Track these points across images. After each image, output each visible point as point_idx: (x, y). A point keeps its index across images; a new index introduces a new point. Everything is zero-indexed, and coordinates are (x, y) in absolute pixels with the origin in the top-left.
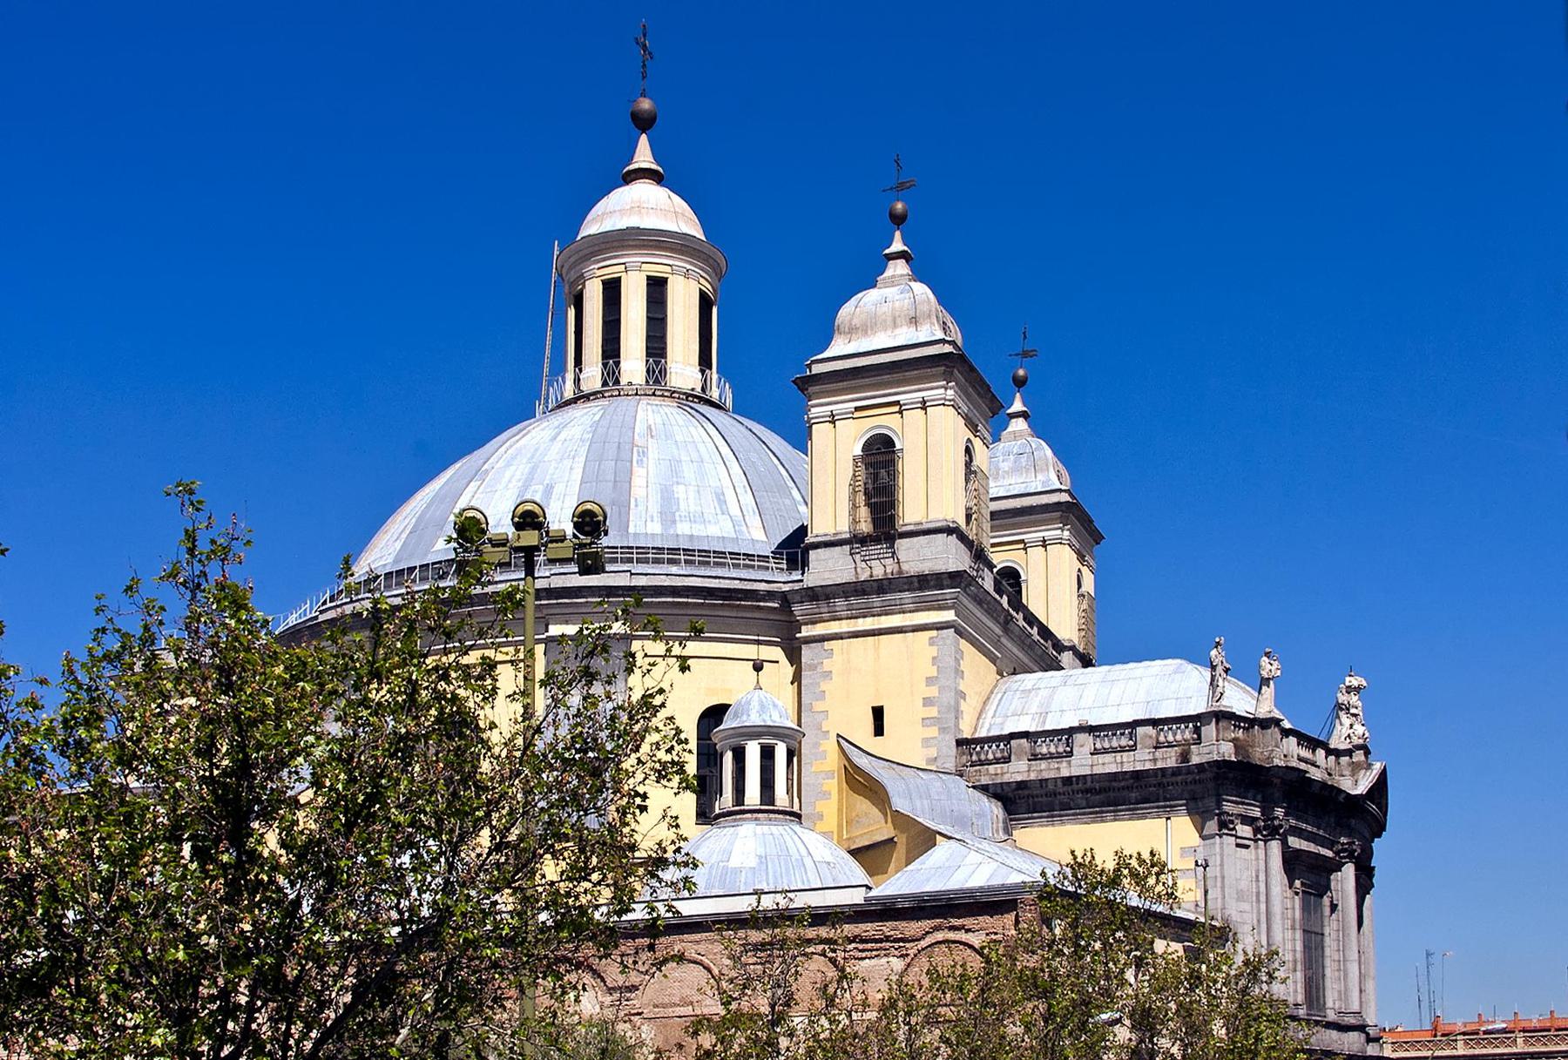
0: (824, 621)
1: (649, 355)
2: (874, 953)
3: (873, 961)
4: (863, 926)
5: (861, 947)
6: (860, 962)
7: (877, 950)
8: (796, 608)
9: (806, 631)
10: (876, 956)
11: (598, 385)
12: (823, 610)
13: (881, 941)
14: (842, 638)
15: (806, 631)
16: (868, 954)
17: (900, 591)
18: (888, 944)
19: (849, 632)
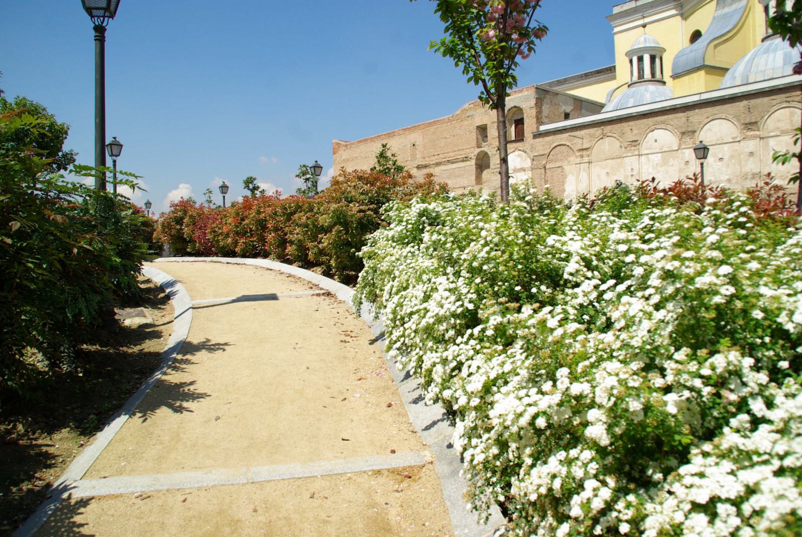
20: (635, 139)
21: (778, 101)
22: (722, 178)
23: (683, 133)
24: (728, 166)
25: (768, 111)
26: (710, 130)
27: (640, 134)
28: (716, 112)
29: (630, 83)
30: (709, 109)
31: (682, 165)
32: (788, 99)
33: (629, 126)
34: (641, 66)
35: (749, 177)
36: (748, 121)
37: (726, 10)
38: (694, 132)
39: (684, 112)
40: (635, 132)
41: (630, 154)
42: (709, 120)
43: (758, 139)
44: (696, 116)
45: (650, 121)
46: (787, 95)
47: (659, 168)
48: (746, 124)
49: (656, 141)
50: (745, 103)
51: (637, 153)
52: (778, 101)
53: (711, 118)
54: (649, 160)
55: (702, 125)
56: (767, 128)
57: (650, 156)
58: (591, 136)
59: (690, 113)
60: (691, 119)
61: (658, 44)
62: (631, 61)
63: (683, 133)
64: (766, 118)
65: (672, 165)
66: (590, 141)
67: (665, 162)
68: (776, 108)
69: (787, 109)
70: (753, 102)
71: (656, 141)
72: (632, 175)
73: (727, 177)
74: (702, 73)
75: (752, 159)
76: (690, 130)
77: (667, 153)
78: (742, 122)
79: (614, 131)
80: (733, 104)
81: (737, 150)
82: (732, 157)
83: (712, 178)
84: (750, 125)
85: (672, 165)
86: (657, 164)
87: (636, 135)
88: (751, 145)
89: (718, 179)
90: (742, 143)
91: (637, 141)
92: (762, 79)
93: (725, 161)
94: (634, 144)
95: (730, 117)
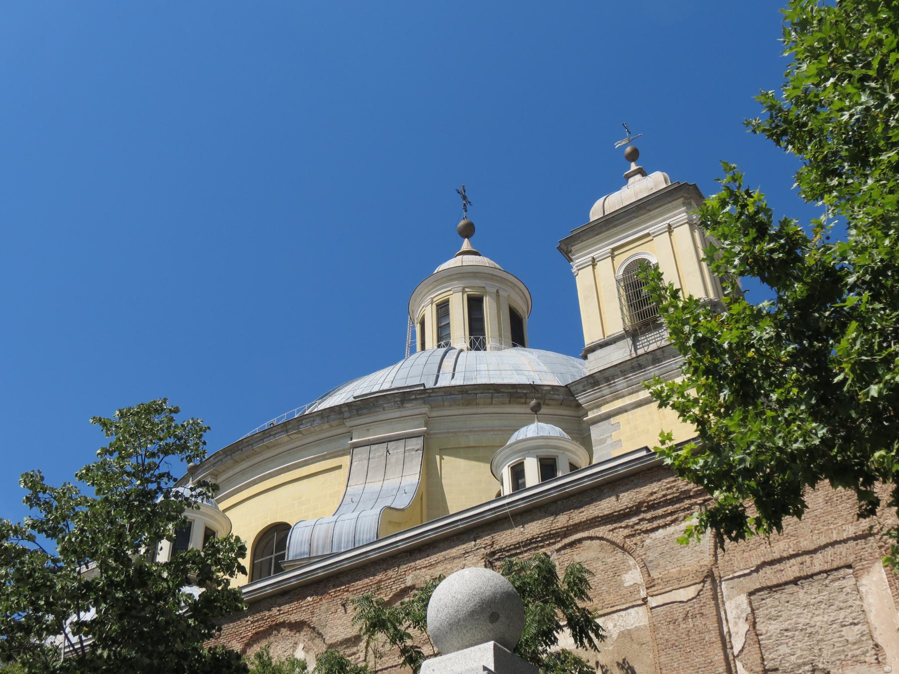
0: (608, 403)
1: (470, 334)
2: (669, 518)
3: (670, 530)
4: (646, 490)
5: (649, 515)
6: (653, 535)
7: (672, 513)
8: (582, 399)
9: (591, 415)
10: (673, 522)
12: (605, 392)
13: (678, 500)
14: (626, 411)
15: (591, 415)
16: (661, 522)
17: (674, 357)
18: (687, 503)
19: (631, 404)
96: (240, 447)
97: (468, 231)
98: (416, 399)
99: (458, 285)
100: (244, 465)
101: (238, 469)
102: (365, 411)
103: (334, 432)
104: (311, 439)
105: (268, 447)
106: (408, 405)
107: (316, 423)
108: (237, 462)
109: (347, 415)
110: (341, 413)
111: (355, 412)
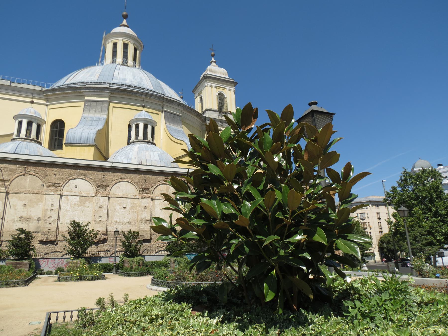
11: (121, 63)
20: (56, 182)
21: (161, 179)
22: (125, 221)
23: (99, 186)
24: (129, 213)
25: (156, 184)
26: (119, 187)
27: (63, 179)
28: (124, 177)
29: (14, 136)
30: (120, 174)
31: (97, 208)
32: (166, 180)
33: (53, 171)
34: (29, 128)
35: (143, 222)
36: (144, 187)
37: (91, 115)
38: (107, 186)
39: (101, 171)
40: (57, 176)
41: (53, 193)
42: (119, 180)
43: (150, 199)
44: (110, 176)
45: (73, 171)
46: (166, 177)
47: (76, 208)
48: (142, 188)
49: (76, 187)
50: (142, 176)
51: (59, 193)
52: (161, 179)
53: (121, 180)
54: (68, 200)
55: (113, 183)
56: (155, 194)
57: (69, 197)
58: (11, 170)
59: (106, 173)
60: (106, 177)
61: (41, 117)
62: (20, 123)
63: (99, 186)
64: (154, 187)
65: (88, 207)
66: (10, 175)
67: (82, 204)
68: (160, 183)
69: (166, 185)
70: (147, 176)
71: (76, 187)
72: (52, 210)
73: (128, 220)
74: (92, 149)
75: (146, 210)
76: (104, 184)
77: (85, 197)
78: (140, 187)
79: (38, 172)
80: (136, 175)
81: (136, 204)
82: (132, 207)
83: (118, 220)
84: (144, 190)
85: (88, 207)
86: (75, 204)
87: (58, 179)
88: (146, 202)
89: (122, 221)
90: (140, 200)
91: (59, 184)
92: (151, 165)
93: (127, 209)
94: (55, 185)
95: (133, 182)
96: (128, 92)
97: (125, 17)
98: (182, 106)
99: (133, 42)
100: (125, 97)
101: (122, 96)
102: (170, 103)
103: (158, 103)
104: (151, 101)
105: (137, 96)
106: (179, 107)
107: (156, 98)
108: (123, 94)
109: (165, 101)
110: (164, 100)
111: (167, 102)
